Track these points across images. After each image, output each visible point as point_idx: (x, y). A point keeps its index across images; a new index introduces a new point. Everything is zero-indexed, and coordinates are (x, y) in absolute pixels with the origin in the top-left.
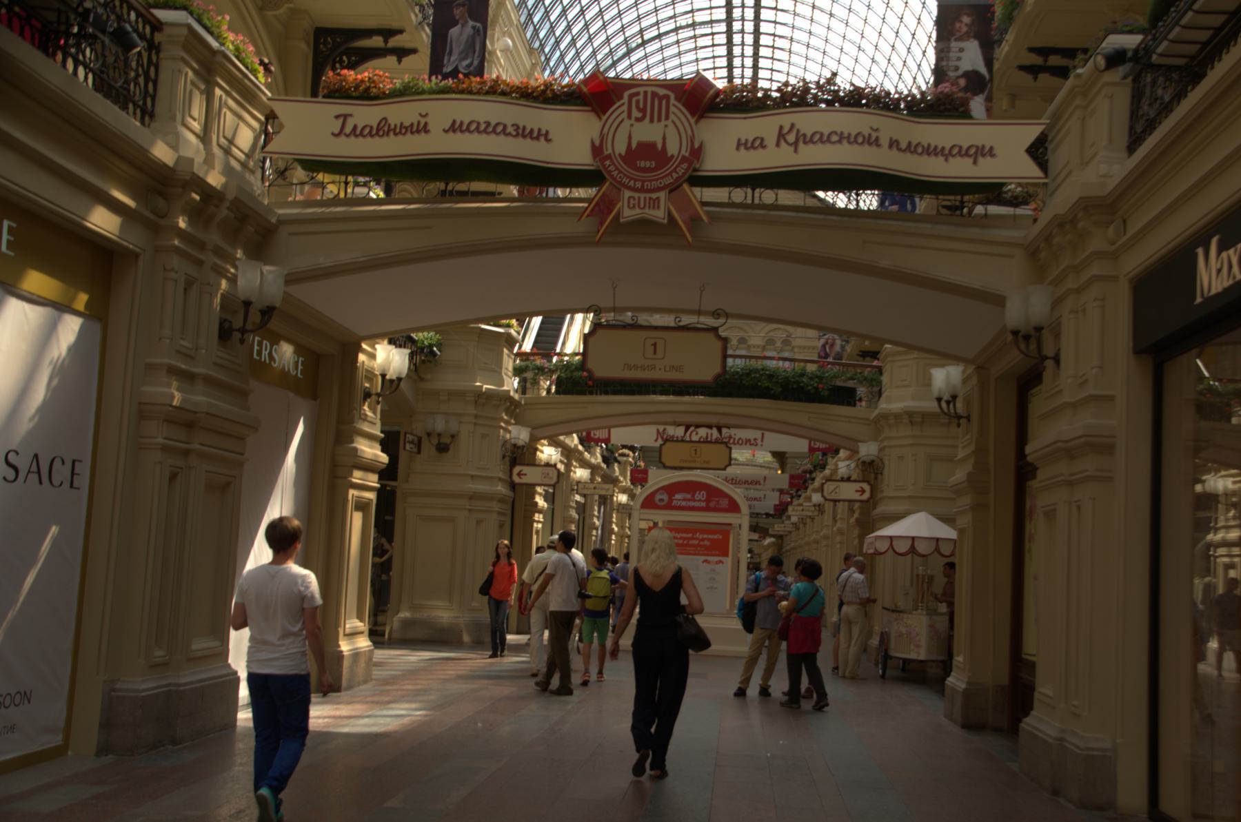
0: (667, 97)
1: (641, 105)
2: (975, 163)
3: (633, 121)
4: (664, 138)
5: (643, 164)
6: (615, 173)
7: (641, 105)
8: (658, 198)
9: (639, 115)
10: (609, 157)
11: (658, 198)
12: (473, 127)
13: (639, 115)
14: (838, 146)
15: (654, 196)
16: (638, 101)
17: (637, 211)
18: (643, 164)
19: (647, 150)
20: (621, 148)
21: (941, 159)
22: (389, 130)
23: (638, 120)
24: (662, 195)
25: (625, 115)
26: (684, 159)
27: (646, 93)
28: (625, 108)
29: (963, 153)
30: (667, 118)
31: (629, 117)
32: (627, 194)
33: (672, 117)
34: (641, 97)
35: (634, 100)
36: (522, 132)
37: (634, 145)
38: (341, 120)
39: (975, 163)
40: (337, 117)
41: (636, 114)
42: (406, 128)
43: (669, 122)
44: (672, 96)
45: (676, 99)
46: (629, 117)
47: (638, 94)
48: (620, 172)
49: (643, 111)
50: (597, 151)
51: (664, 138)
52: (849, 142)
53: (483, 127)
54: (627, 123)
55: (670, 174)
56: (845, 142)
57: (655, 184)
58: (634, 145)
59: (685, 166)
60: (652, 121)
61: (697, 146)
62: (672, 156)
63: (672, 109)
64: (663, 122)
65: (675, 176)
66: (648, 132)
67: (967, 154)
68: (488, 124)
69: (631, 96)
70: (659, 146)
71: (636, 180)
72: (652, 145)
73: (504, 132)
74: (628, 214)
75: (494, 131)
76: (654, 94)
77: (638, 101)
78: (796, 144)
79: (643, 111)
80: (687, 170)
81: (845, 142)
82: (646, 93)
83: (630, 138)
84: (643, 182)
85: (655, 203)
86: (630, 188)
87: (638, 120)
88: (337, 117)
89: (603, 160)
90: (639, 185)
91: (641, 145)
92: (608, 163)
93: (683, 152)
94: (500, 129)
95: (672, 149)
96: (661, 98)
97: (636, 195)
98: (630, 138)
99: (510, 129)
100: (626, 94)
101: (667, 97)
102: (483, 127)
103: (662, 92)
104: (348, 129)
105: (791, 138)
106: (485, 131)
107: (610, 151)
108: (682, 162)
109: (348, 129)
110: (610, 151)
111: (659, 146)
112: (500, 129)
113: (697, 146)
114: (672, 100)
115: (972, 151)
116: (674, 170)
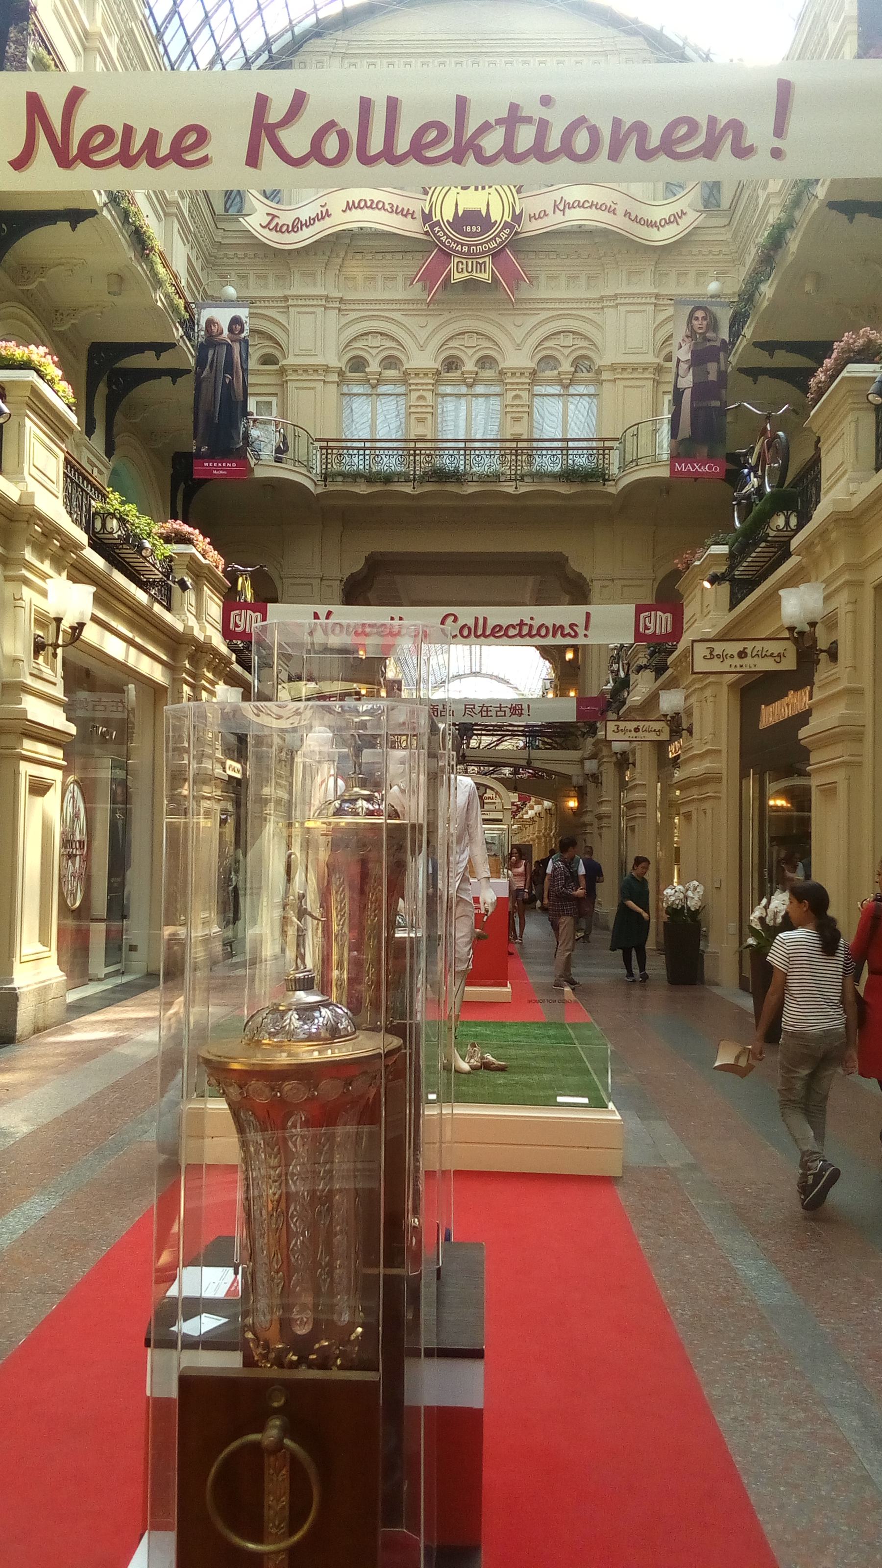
14: (589, 209)
22: (302, 226)
38: (270, 217)
40: (268, 214)
42: (314, 219)
52: (596, 208)
53: (369, 204)
56: (594, 207)
74: (457, 277)
78: (564, 211)
81: (594, 207)
88: (268, 214)
90: (465, 249)
97: (464, 261)
102: (369, 204)
105: (561, 207)
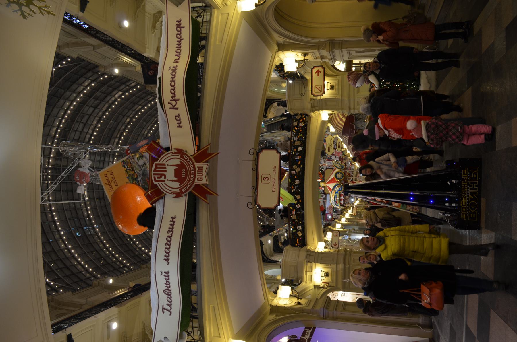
0: (156, 165)
2: (183, 27)
4: (173, 166)
6: (188, 187)
8: (198, 167)
9: (163, 177)
10: (181, 190)
11: (198, 167)
12: (167, 251)
13: (163, 177)
15: (197, 169)
16: (158, 178)
17: (204, 176)
19: (177, 173)
20: (177, 185)
21: (182, 41)
23: (165, 178)
24: (197, 166)
26: (182, 157)
27: (154, 174)
28: (160, 183)
29: (179, 33)
30: (164, 164)
31: (164, 181)
32: (196, 181)
33: (164, 162)
34: (156, 176)
35: (157, 179)
36: (171, 229)
37: (176, 179)
39: (183, 27)
43: (166, 164)
44: (156, 162)
45: (157, 161)
46: (164, 181)
47: (154, 178)
49: (162, 175)
50: (178, 195)
51: (173, 166)
54: (166, 182)
55: (188, 162)
58: (176, 179)
60: (166, 171)
61: (176, 151)
63: (161, 162)
64: (166, 166)
66: (170, 173)
67: (180, 31)
68: (166, 244)
69: (156, 181)
70: (176, 167)
72: (175, 170)
73: (170, 237)
75: (170, 241)
76: (155, 171)
77: (158, 178)
79: (162, 175)
82: (154, 174)
83: (173, 181)
84: (191, 174)
85: (200, 169)
87: (165, 178)
89: (183, 193)
90: (192, 176)
91: (175, 176)
92: (183, 190)
93: (179, 157)
94: (169, 239)
95: (177, 162)
96: (156, 168)
97: (197, 177)
98: (173, 181)
99: (169, 234)
100: (155, 183)
101: (156, 165)
103: (154, 167)
104: (169, 308)
106: (169, 245)
107: (178, 190)
108: (183, 157)
109: (169, 308)
110: (178, 190)
111: (176, 167)
112: (169, 239)
113: (176, 151)
115: (179, 29)
116: (186, 160)
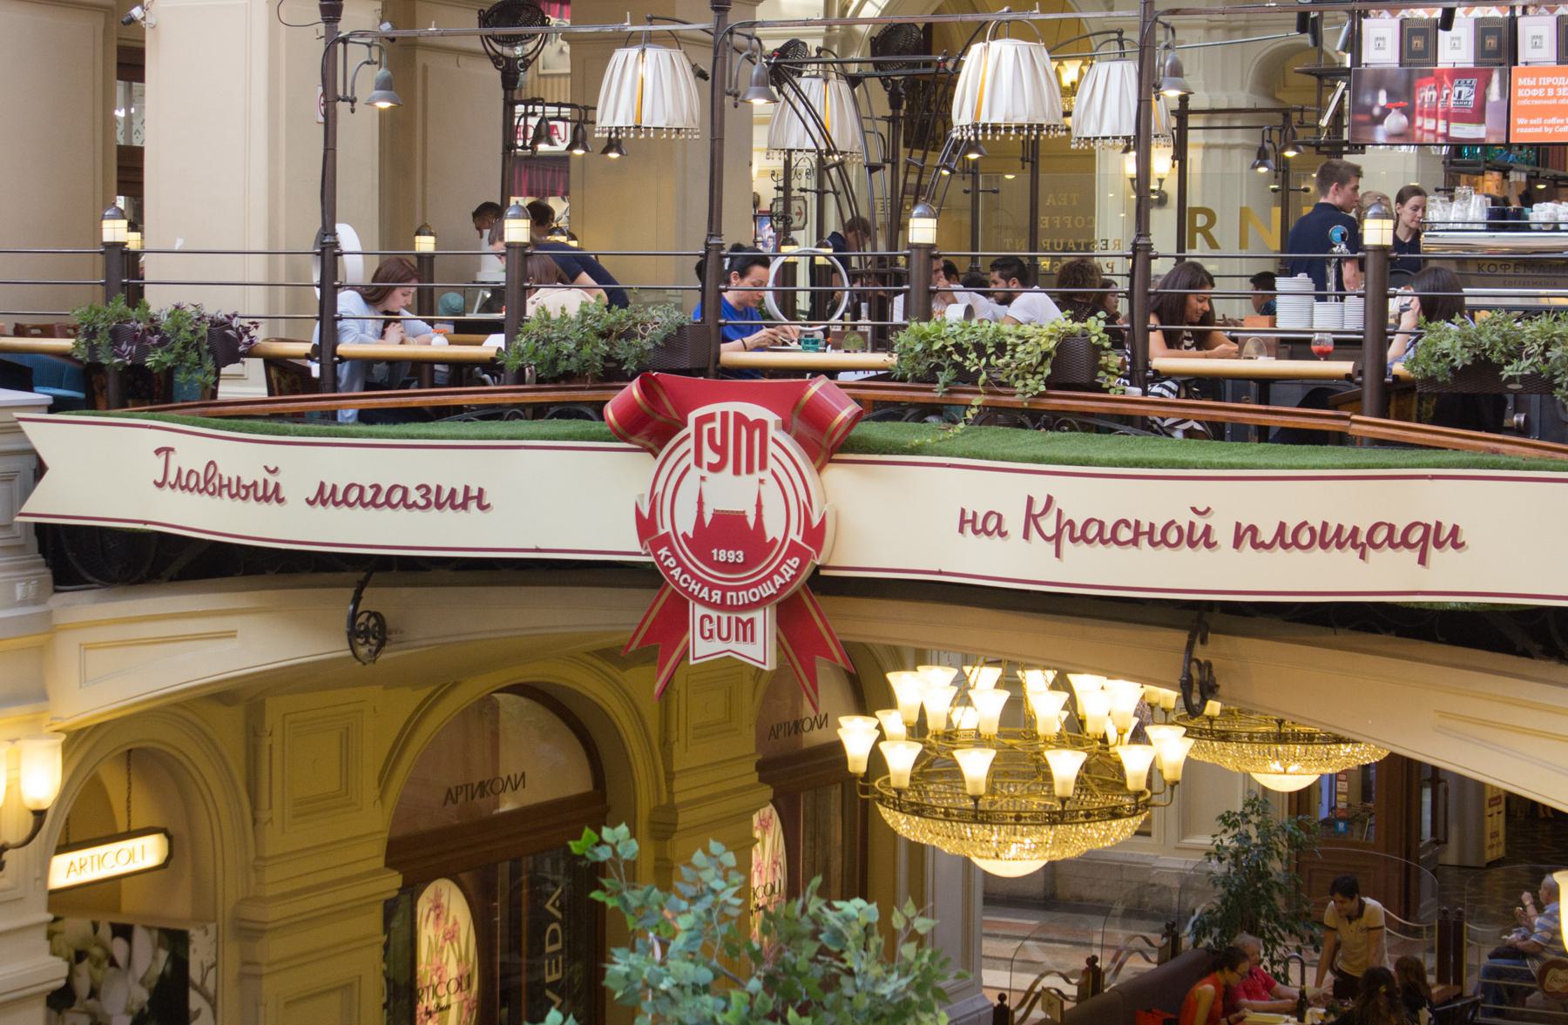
1: (718, 442)
3: (705, 472)
4: (759, 506)
5: (721, 555)
7: (718, 442)
8: (751, 621)
11: (751, 621)
15: (745, 617)
16: (712, 432)
18: (721, 555)
20: (686, 525)
23: (714, 468)
24: (758, 615)
25: (690, 458)
28: (690, 444)
30: (763, 466)
31: (698, 462)
34: (717, 425)
35: (706, 427)
37: (708, 519)
41: (710, 456)
43: (766, 475)
46: (698, 462)
48: (685, 570)
49: (721, 450)
50: (646, 526)
51: (759, 506)
54: (695, 472)
55: (769, 577)
57: (745, 597)
58: (708, 519)
59: (795, 562)
60: (737, 471)
61: (816, 521)
62: (774, 541)
63: (772, 448)
64: (758, 474)
65: (778, 580)
70: (751, 521)
71: (712, 587)
72: (740, 518)
76: (740, 418)
77: (712, 432)
80: (799, 569)
82: (725, 415)
83: (700, 503)
85: (746, 631)
86: (702, 601)
90: (717, 596)
91: (719, 517)
92: (663, 552)
95: (774, 529)
97: (714, 614)
98: (700, 503)
100: (692, 417)
101: (762, 424)
107: (668, 528)
108: (789, 555)
110: (668, 528)
111: (751, 521)
113: (816, 521)
114: (772, 432)
116: (776, 571)
